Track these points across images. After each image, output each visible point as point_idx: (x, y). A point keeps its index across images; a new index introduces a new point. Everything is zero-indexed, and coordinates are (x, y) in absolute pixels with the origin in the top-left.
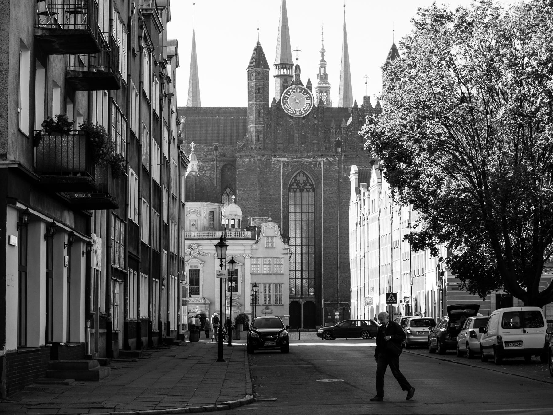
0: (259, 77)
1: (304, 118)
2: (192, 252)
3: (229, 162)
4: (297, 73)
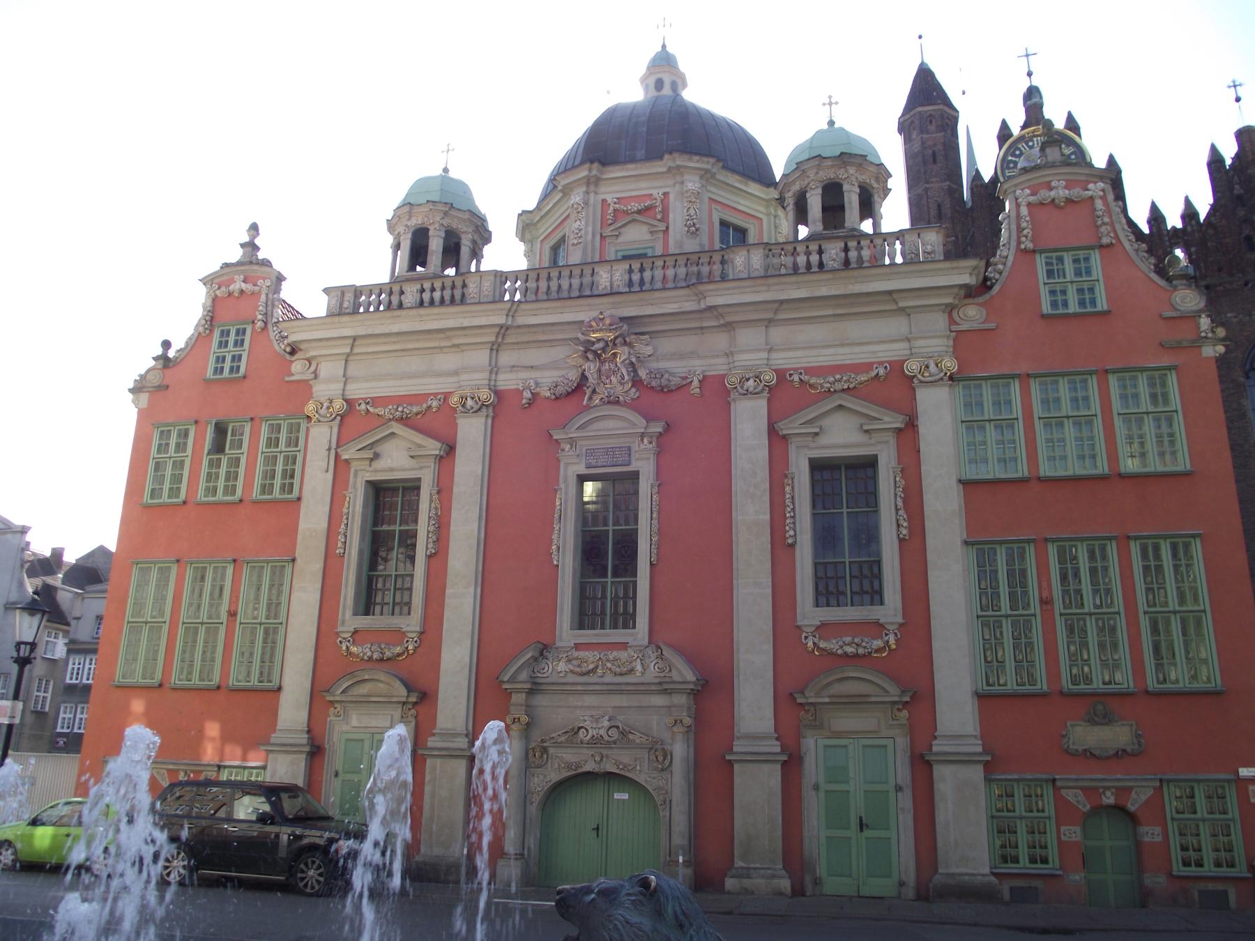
0: (932, 128)
2: (591, 368)
4: (1035, 100)
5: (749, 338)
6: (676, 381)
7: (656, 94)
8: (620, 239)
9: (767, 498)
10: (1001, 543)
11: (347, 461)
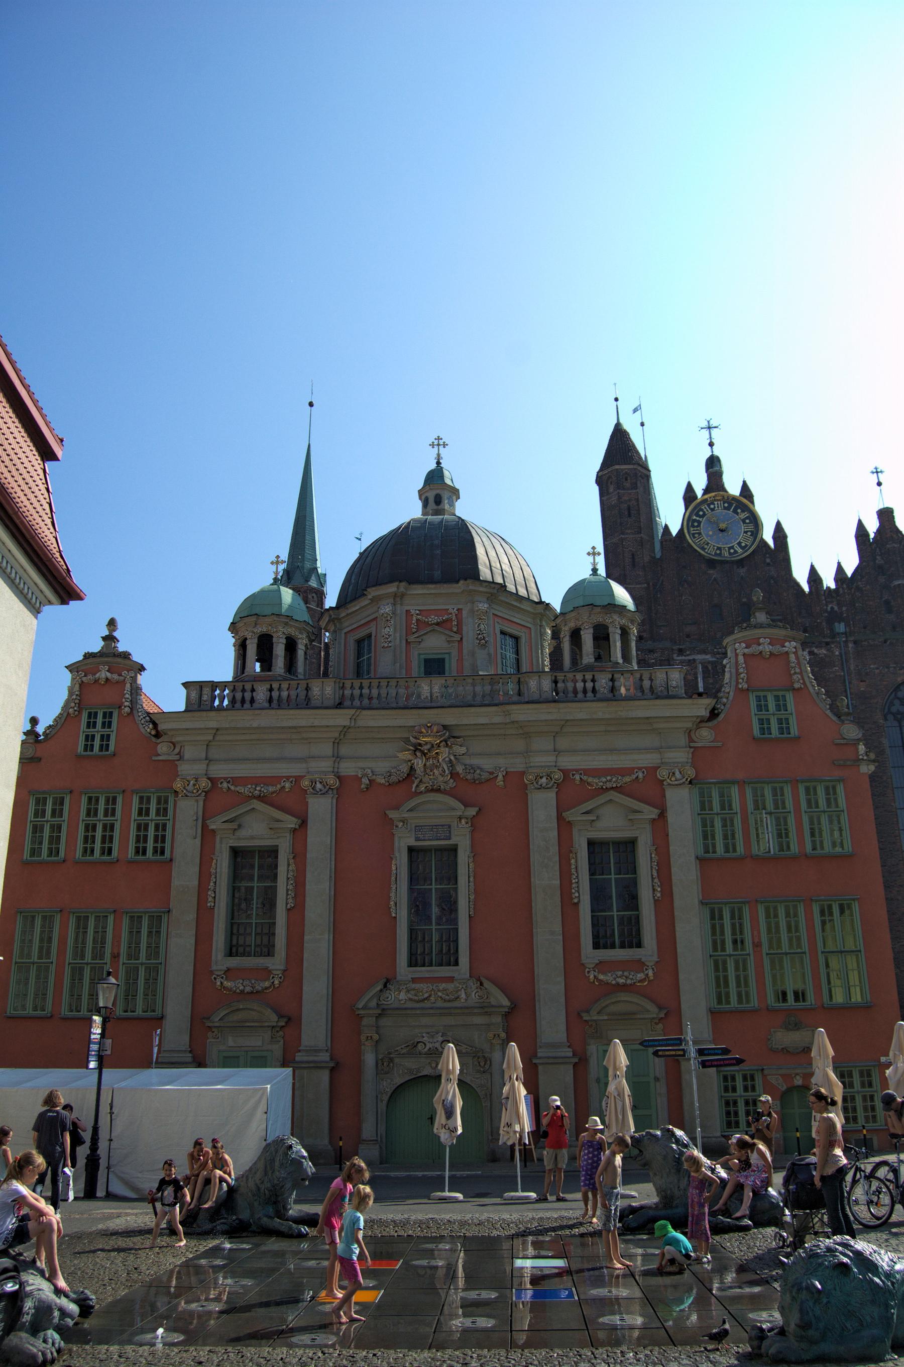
0: (627, 485)
1: (741, 563)
2: (419, 763)
6: (485, 776)
8: (422, 645)
9: (557, 867)
10: (726, 904)
11: (213, 831)
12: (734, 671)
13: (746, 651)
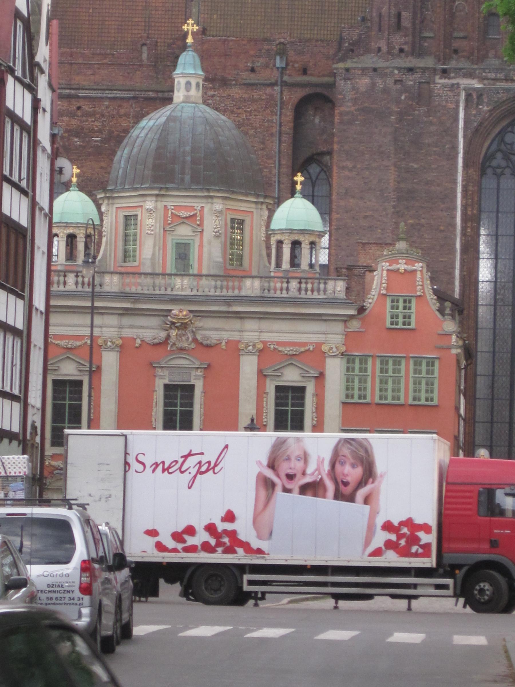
2: (174, 333)
3: (319, 90)
5: (251, 325)
6: (215, 342)
7: (186, 93)
9: (255, 403)
12: (379, 281)
13: (389, 268)
